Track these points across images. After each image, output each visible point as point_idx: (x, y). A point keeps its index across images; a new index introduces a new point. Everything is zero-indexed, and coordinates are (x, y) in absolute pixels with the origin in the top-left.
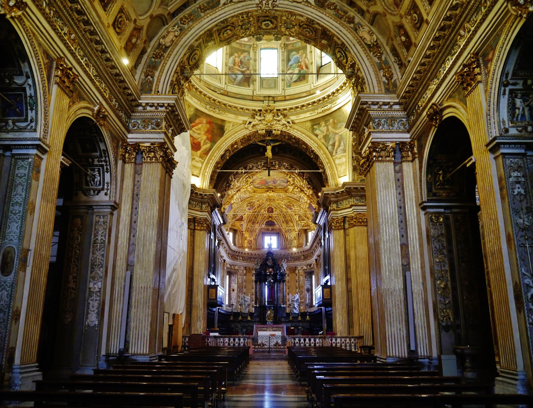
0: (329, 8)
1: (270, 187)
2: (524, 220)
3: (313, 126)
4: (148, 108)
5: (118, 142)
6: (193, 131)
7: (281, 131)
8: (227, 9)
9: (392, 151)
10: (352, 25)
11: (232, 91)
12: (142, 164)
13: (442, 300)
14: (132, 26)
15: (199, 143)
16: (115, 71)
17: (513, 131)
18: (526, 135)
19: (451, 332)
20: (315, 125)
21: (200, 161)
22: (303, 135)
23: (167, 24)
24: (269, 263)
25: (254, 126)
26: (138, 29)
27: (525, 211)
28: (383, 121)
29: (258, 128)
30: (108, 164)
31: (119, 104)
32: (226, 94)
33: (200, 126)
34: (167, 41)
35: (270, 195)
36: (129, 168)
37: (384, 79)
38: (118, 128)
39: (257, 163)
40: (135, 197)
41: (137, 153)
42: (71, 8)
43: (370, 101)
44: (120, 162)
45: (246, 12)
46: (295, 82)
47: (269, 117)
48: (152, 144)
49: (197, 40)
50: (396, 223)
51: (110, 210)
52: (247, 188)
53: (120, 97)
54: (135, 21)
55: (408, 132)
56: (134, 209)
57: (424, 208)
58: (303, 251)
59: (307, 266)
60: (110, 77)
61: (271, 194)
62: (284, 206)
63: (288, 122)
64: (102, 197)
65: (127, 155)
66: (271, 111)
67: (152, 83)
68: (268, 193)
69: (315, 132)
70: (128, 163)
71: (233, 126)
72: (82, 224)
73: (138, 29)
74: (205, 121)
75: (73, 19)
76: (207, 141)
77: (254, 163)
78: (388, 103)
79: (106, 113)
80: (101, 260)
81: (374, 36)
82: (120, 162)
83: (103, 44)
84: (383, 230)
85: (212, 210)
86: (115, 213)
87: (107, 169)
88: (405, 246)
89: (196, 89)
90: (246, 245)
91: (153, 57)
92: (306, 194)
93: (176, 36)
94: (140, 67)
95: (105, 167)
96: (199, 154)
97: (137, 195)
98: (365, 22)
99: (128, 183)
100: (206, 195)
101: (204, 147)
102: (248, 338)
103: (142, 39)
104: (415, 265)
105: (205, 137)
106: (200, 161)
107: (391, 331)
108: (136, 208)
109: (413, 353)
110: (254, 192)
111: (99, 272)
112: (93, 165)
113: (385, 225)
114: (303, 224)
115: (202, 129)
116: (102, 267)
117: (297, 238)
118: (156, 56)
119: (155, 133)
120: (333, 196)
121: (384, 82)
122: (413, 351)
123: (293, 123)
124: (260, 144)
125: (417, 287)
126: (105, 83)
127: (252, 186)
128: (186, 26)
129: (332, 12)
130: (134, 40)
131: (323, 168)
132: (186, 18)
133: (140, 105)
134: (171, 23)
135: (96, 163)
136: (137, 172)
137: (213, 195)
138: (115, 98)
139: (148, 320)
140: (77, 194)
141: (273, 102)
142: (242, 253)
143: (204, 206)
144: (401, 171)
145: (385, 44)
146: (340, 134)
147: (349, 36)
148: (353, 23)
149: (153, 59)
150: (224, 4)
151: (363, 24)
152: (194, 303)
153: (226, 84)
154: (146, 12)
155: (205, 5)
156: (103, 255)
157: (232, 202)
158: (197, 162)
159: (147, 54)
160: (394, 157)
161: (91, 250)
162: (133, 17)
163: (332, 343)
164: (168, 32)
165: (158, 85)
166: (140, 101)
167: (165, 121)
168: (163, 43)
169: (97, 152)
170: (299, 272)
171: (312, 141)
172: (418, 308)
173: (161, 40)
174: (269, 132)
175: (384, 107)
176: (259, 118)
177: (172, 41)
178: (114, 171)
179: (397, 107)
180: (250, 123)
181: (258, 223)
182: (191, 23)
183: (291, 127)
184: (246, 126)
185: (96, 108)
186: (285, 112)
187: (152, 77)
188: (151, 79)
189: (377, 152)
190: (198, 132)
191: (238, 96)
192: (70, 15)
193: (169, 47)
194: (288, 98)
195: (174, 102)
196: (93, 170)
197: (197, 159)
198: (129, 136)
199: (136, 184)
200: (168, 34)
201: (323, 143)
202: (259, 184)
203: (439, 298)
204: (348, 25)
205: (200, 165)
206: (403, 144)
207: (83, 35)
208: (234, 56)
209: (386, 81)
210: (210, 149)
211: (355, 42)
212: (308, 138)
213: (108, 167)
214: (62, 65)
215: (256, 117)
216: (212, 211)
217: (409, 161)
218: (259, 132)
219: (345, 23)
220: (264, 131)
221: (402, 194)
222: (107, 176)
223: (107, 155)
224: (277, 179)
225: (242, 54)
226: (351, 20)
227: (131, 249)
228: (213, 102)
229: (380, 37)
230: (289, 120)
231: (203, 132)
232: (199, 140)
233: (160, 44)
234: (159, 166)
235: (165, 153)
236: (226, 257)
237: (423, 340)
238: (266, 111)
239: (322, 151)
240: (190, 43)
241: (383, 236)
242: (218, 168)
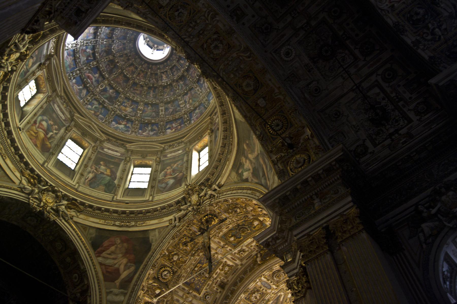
3: (237, 172)
6: (104, 257)
15: (118, 270)
21: (122, 293)
33: (113, 248)
71: (160, 233)
76: (129, 264)
105: (125, 261)
106: (122, 293)
146: (259, 152)
158: (116, 295)
171: (245, 191)
197: (116, 291)
210: (135, 273)
215: (182, 207)
231: (121, 255)
232: (117, 266)
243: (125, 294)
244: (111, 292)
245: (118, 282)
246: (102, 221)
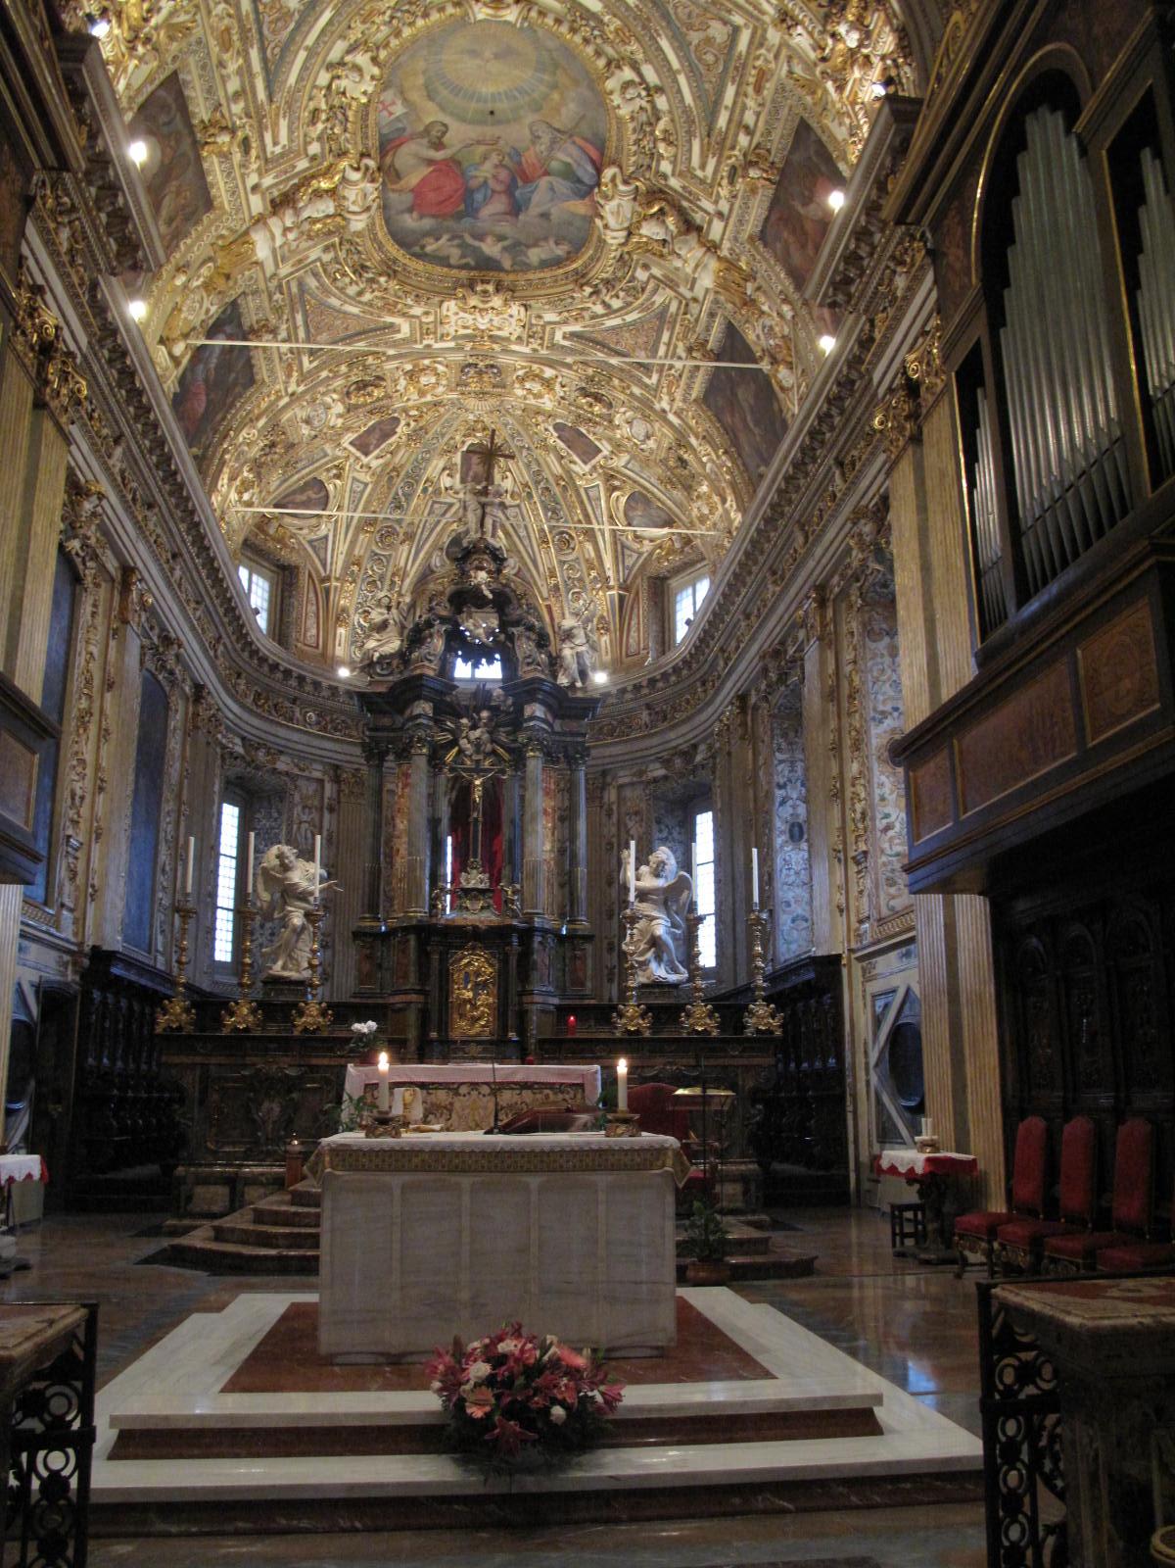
58: (652, 682)
59: (666, 763)
62: (553, 439)
90: (340, 651)
92: (712, 248)
114: (647, 546)
117: (614, 623)
142: (317, 685)
170: (620, 799)
181: (409, 537)
224: (530, 157)
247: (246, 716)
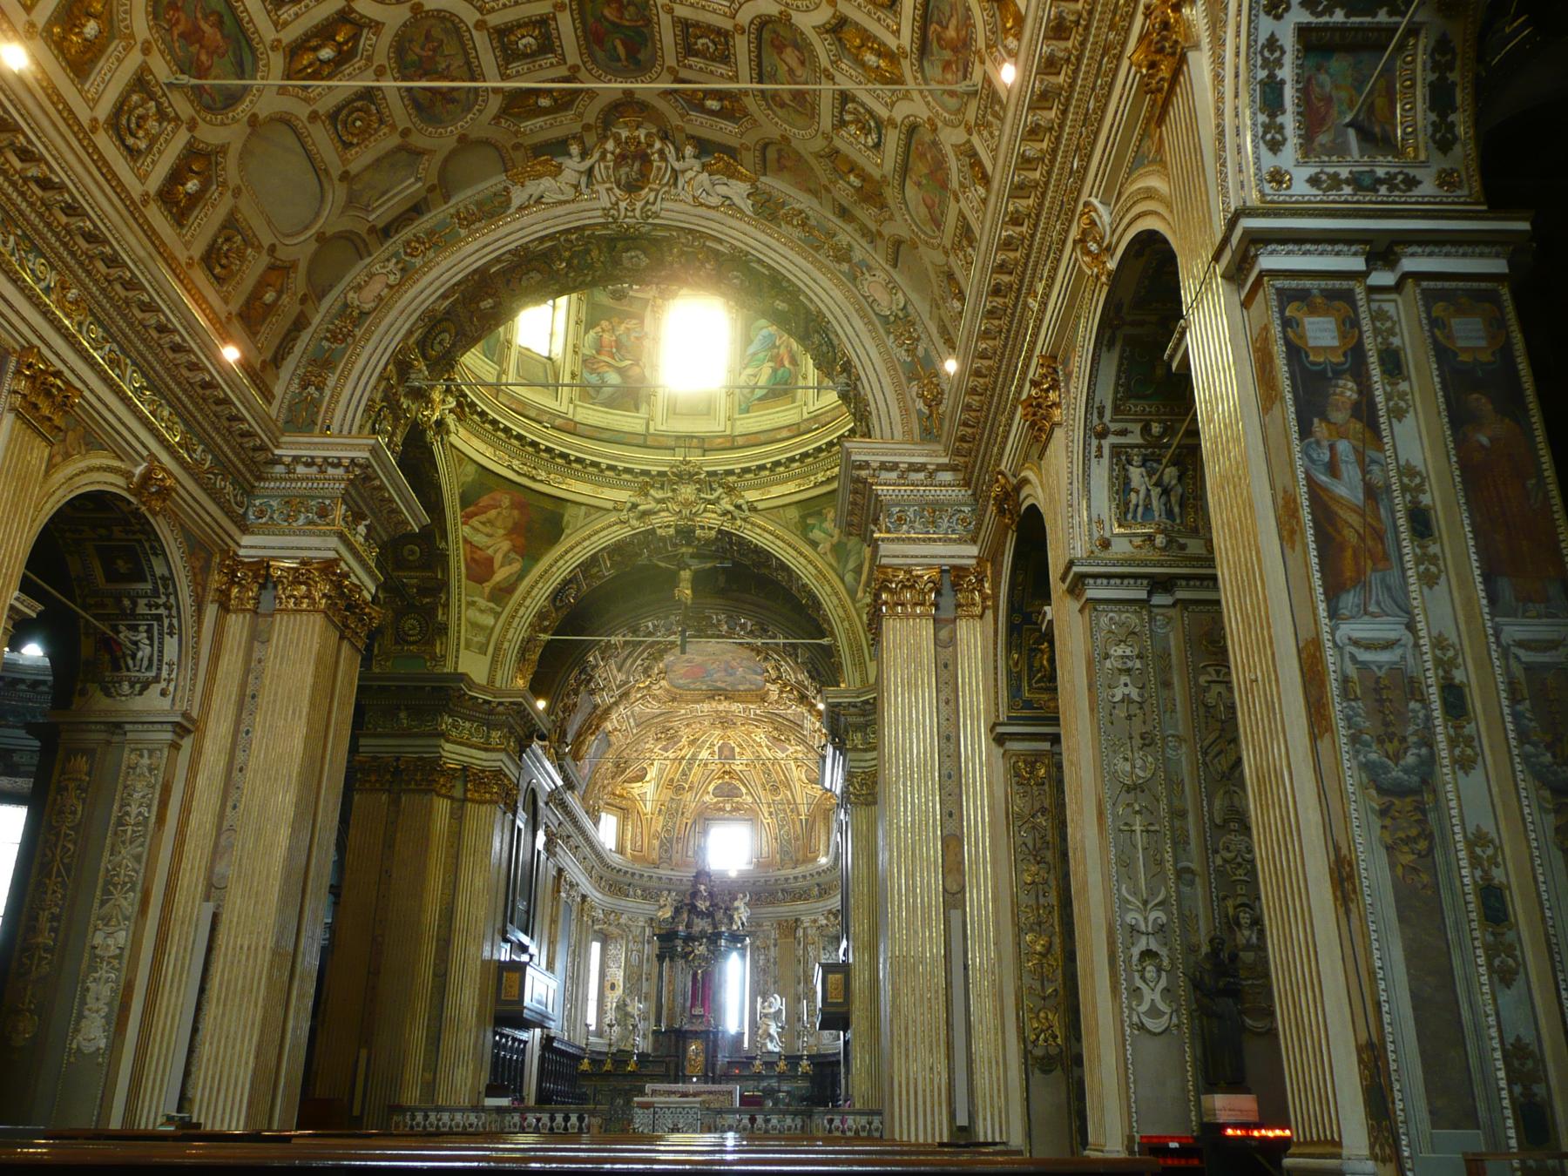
0: (789, 223)
1: (719, 684)
2: (1138, 766)
3: (803, 518)
4: (300, 469)
5: (211, 555)
7: (720, 531)
8: (526, 220)
9: (931, 590)
10: (845, 267)
11: (590, 422)
12: (272, 615)
13: (1037, 985)
14: (265, 260)
15: (491, 560)
16: (197, 377)
17: (1121, 548)
18: (1155, 556)
19: (1058, 1072)
20: (810, 515)
22: (778, 542)
23: (370, 255)
24: (702, 905)
25: (645, 514)
26: (279, 270)
27: (1138, 742)
28: (911, 513)
29: (656, 521)
30: (174, 612)
31: (215, 457)
32: (572, 428)
33: (493, 513)
34: (366, 299)
35: (721, 708)
36: (237, 625)
37: (920, 404)
38: (208, 519)
39: (667, 617)
40: (246, 701)
41: (263, 587)
42: (66, 227)
43: (875, 460)
44: (211, 611)
45: (577, 229)
46: (760, 399)
47: (687, 491)
48: (304, 563)
49: (444, 296)
50: (933, 779)
51: (169, 736)
52: (648, 687)
53: (219, 440)
54: (272, 249)
55: (974, 541)
56: (240, 734)
57: (1000, 740)
60: (185, 391)
61: (724, 706)
63: (739, 507)
64: (153, 702)
65: (235, 591)
66: (691, 475)
67: (316, 404)
68: (714, 704)
69: (811, 535)
70: (235, 612)
71: (587, 515)
72: (89, 774)
73: (279, 270)
74: (506, 502)
75: (73, 254)
76: (513, 555)
77: (658, 618)
78: (921, 468)
79: (168, 483)
80: (134, 870)
81: (900, 294)
82: (211, 611)
83: (160, 310)
84: (898, 797)
85: (523, 746)
86: (187, 743)
87: (171, 626)
88: (952, 842)
89: (483, 414)
91: (326, 339)
93: (390, 287)
94: (290, 363)
95: (166, 622)
96: (487, 590)
97: (254, 697)
98: (879, 259)
99: (231, 663)
100: (500, 704)
101: (501, 575)
102: (592, 1114)
103: (295, 294)
104: (981, 897)
105: (506, 545)
106: (491, 610)
107: (907, 1071)
108: (247, 732)
109: (963, 1137)
110: (673, 700)
111: (125, 904)
112: (134, 615)
113: (905, 785)
115: (498, 523)
116: (132, 889)
118: (335, 337)
119: (313, 534)
120: (852, 710)
121: (919, 412)
122: (962, 1129)
123: (753, 509)
124: (662, 564)
125: (979, 957)
126: (170, 405)
127: (663, 683)
128: (418, 262)
129: (796, 233)
130: (269, 297)
131: (832, 634)
132: (418, 240)
133: (277, 461)
134: (380, 253)
135: (142, 609)
136: (257, 636)
137: (520, 704)
138: (201, 441)
139: (250, 1040)
140: (83, 693)
141: (700, 452)
142: (642, 876)
143: (496, 734)
144: (953, 641)
145: (926, 317)
147: (837, 294)
148: (849, 261)
149: (325, 344)
150: (521, 208)
151: (872, 263)
152: (449, 1011)
153: (571, 401)
154: (306, 228)
155: (473, 207)
156: (138, 858)
157: (609, 726)
158: (482, 611)
159: (311, 329)
160: (936, 605)
161: (108, 841)
162: (267, 239)
163: (830, 1131)
164: (371, 276)
165: (330, 410)
166: (277, 452)
167: (344, 502)
168: (356, 303)
169: (145, 580)
170: (805, 935)
171: (802, 560)
172: (983, 1009)
173: (351, 295)
174: (686, 534)
175: (914, 476)
176: (660, 495)
177: (380, 298)
178: (191, 632)
179: (947, 476)
180: (635, 506)
182: (431, 254)
183: (744, 520)
184: (624, 516)
185: (138, 471)
186: (731, 479)
187: (320, 389)
188: (316, 395)
189: (890, 591)
190: (487, 530)
191: (605, 435)
192: (65, 245)
193: (368, 314)
194: (740, 441)
195: (367, 455)
196: (134, 628)
197: (483, 603)
198: (246, 540)
199: (251, 667)
200: (369, 278)
201: (831, 565)
202: (685, 676)
203: (1027, 980)
204: (834, 266)
205: (488, 620)
206: (958, 572)
207: (103, 291)
208: (598, 329)
209: (926, 410)
210: (521, 576)
211: (850, 310)
212: (790, 550)
213: (175, 621)
214: (30, 366)
215: (652, 492)
216: (522, 751)
217: (972, 617)
218: (659, 531)
219: (827, 262)
220: (672, 531)
221: (952, 704)
222: (171, 645)
223: (171, 589)
225: (621, 322)
226: (843, 255)
227: (223, 842)
228: (530, 449)
229: (913, 296)
230: (741, 501)
231: (501, 532)
232: (490, 552)
233: (346, 305)
234: (319, 619)
235: (338, 586)
236: (586, 886)
237: (992, 1097)
238: (680, 475)
239: (827, 588)
240: (424, 307)
241: (898, 814)
242: (545, 630)
243: (497, 615)
244: (473, 603)
245: (488, 587)
246: (489, 452)
247: (606, 899)
